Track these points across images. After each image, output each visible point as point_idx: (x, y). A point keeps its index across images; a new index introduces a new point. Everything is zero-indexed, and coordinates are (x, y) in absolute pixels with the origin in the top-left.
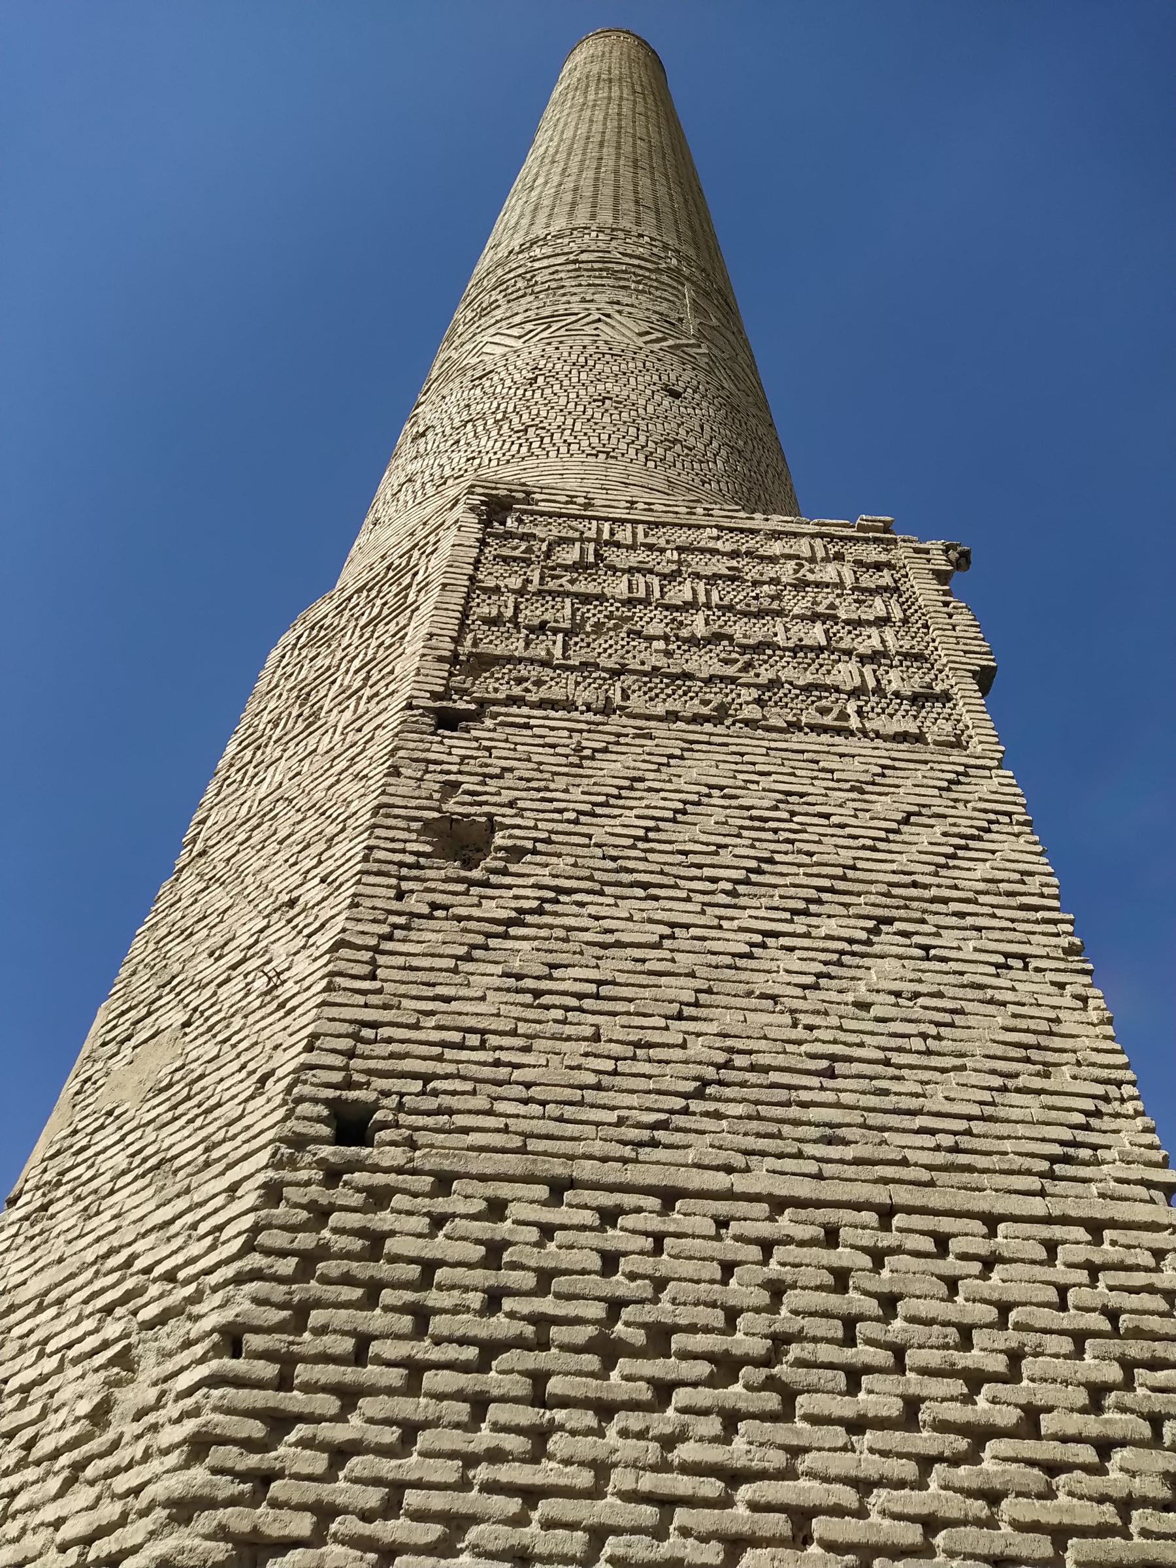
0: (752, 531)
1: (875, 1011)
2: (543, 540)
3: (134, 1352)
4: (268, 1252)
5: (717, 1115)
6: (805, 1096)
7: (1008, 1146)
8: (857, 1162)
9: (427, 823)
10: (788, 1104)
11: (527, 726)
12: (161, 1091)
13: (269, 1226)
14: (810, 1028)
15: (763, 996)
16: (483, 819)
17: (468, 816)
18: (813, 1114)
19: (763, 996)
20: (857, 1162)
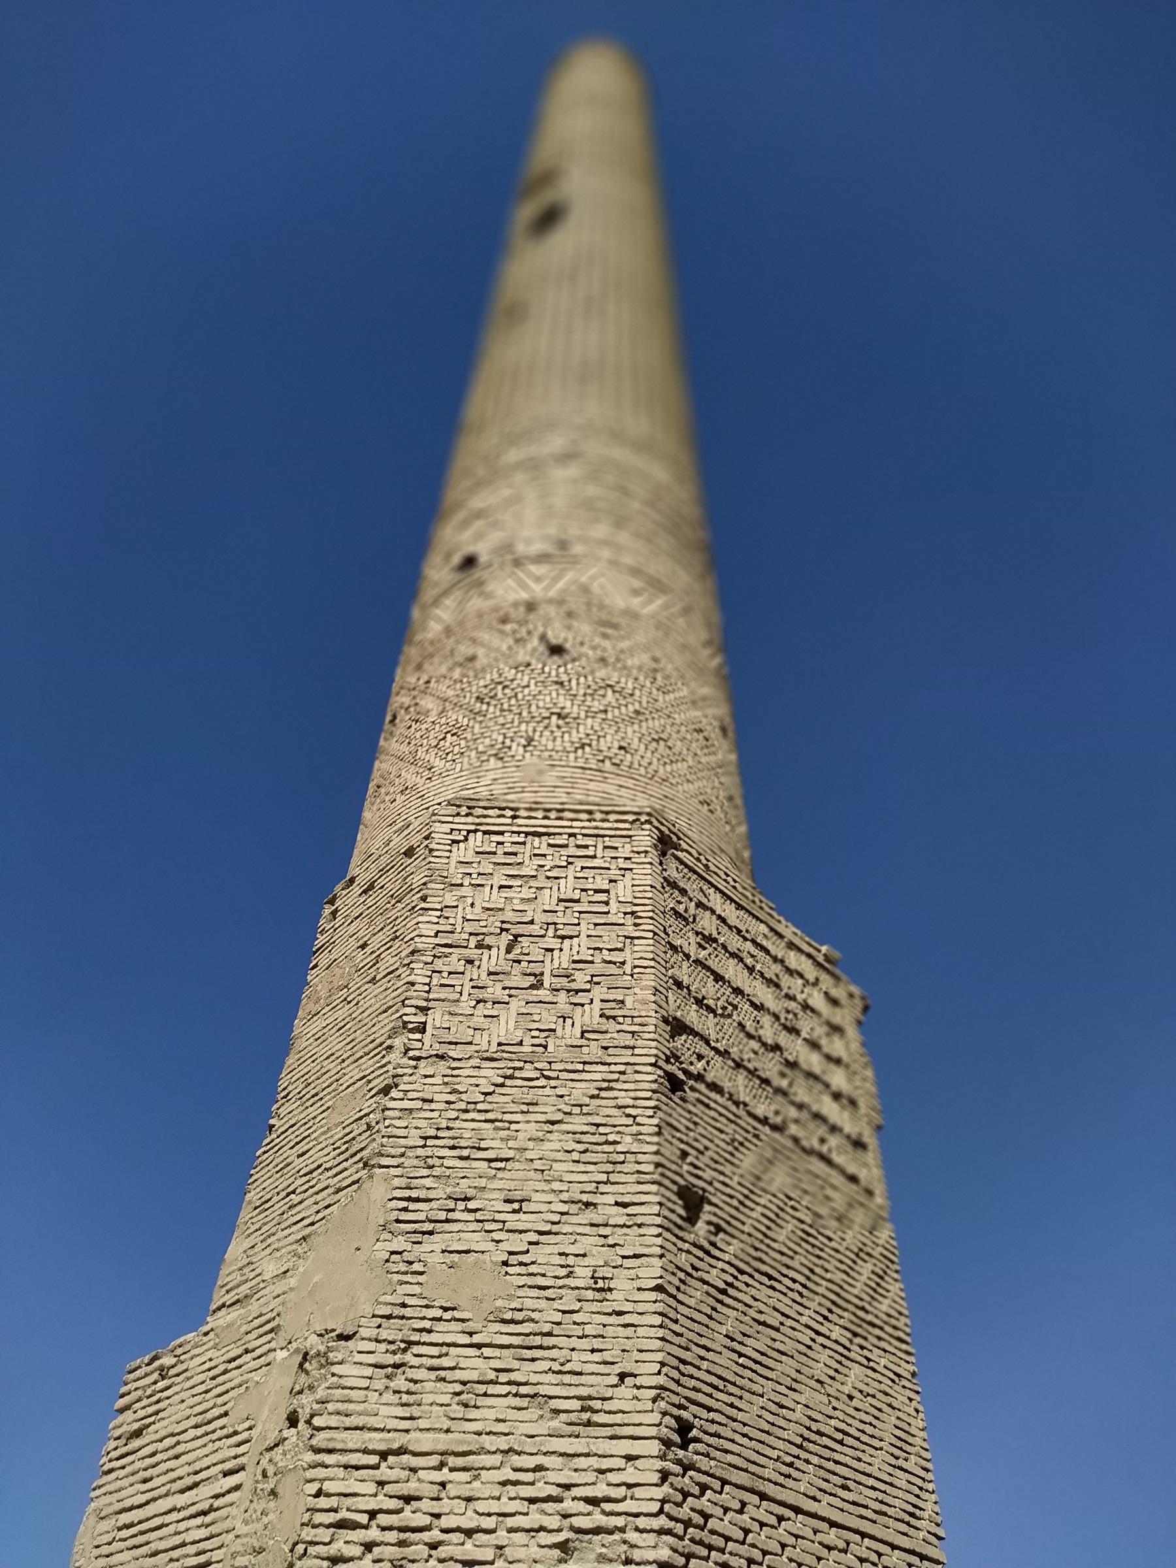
0: (781, 936)
1: (855, 1403)
2: (691, 900)
3: (571, 1544)
4: (671, 1518)
5: (807, 1462)
6: (837, 1457)
7: (897, 1502)
8: (854, 1503)
9: (680, 1187)
10: (829, 1460)
11: (707, 1106)
12: (504, 1321)
13: (669, 1501)
14: (835, 1409)
15: (818, 1381)
16: (701, 1192)
17: (694, 1186)
18: (839, 1469)
19: (818, 1381)
20: (854, 1503)
